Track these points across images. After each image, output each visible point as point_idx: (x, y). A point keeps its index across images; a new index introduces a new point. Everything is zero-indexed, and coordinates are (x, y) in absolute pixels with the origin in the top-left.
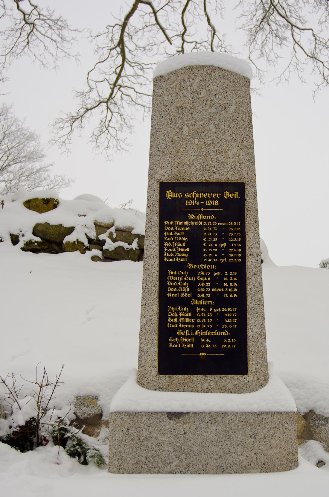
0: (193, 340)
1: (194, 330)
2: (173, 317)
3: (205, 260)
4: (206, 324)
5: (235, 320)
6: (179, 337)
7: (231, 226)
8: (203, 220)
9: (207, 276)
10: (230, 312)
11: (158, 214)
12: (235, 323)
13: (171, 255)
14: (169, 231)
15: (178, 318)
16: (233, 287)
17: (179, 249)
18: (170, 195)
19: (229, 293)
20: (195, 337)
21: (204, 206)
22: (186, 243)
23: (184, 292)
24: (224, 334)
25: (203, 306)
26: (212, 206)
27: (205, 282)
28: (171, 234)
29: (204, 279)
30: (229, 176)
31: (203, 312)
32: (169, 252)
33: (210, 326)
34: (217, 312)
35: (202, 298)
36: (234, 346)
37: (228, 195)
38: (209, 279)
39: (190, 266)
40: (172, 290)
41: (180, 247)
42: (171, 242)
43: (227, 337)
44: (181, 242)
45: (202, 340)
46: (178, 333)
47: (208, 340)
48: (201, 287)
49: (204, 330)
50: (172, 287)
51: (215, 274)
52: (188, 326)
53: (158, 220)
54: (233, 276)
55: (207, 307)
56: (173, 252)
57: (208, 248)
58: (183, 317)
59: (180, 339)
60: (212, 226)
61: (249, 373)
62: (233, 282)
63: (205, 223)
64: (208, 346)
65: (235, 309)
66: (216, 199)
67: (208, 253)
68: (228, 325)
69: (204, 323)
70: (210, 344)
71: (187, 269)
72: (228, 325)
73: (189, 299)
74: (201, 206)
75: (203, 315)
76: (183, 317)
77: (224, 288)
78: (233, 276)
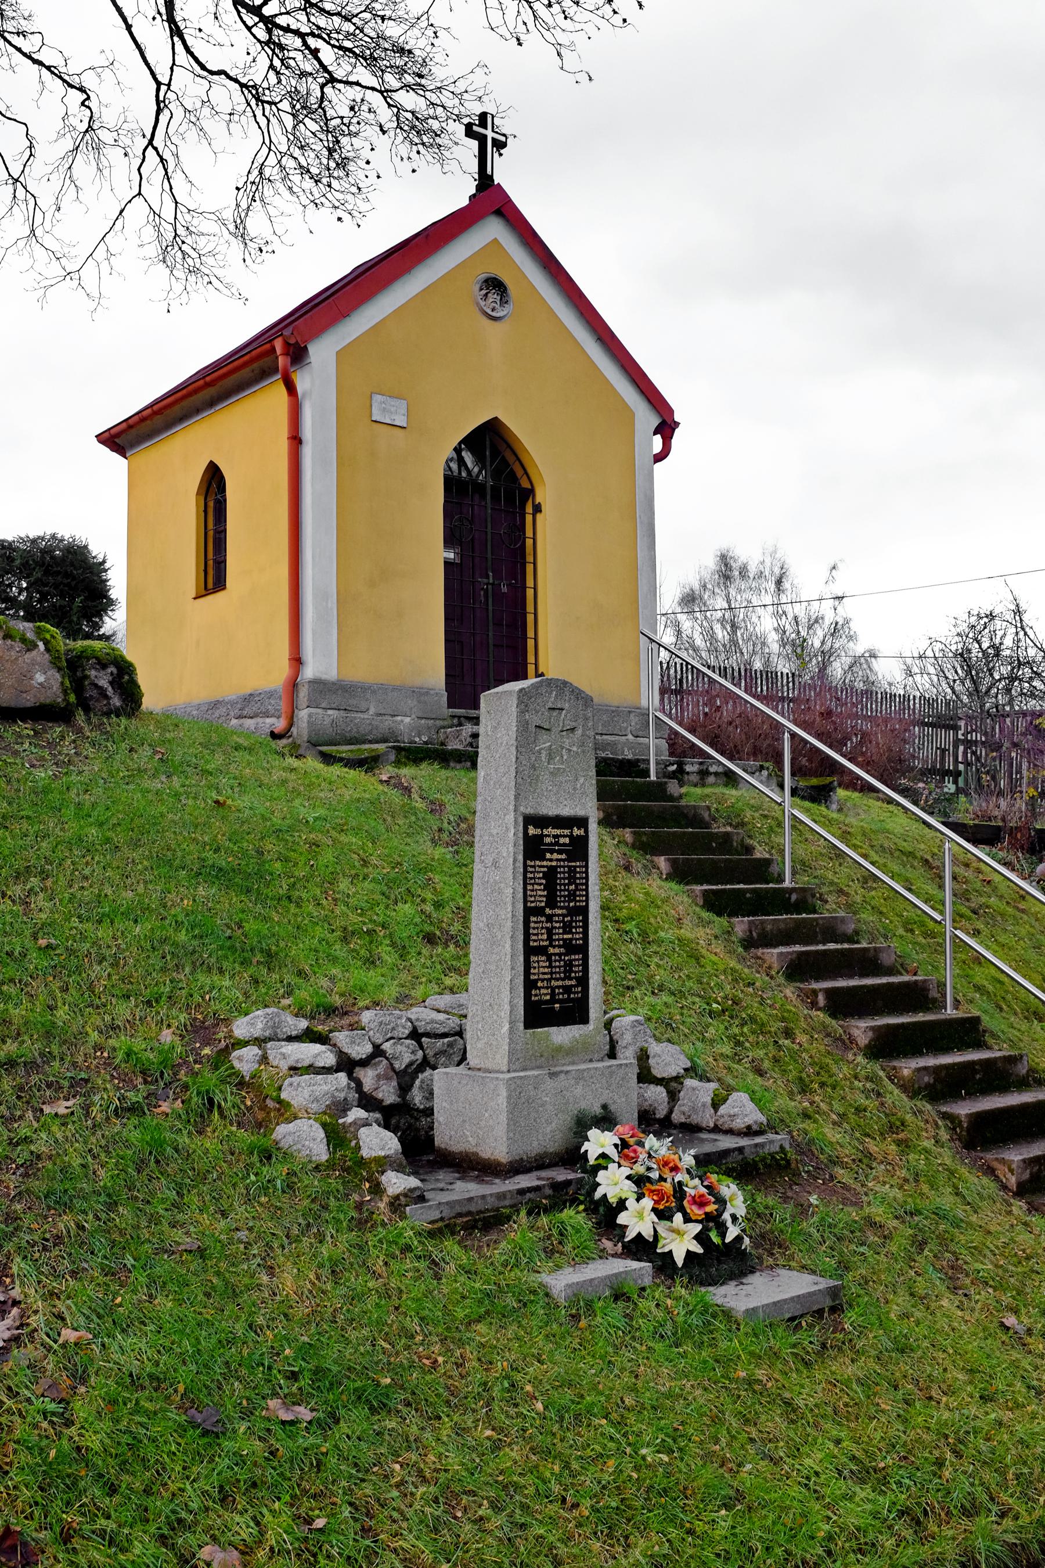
8: (557, 860)
17: (539, 893)
18: (532, 831)
19: (576, 939)
21: (557, 843)
26: (564, 845)
29: (557, 925)
33: (562, 975)
37: (576, 832)
39: (548, 911)
44: (540, 884)
49: (557, 979)
55: (560, 955)
60: (564, 867)
61: (591, 1022)
71: (543, 914)
73: (546, 947)
74: (557, 843)
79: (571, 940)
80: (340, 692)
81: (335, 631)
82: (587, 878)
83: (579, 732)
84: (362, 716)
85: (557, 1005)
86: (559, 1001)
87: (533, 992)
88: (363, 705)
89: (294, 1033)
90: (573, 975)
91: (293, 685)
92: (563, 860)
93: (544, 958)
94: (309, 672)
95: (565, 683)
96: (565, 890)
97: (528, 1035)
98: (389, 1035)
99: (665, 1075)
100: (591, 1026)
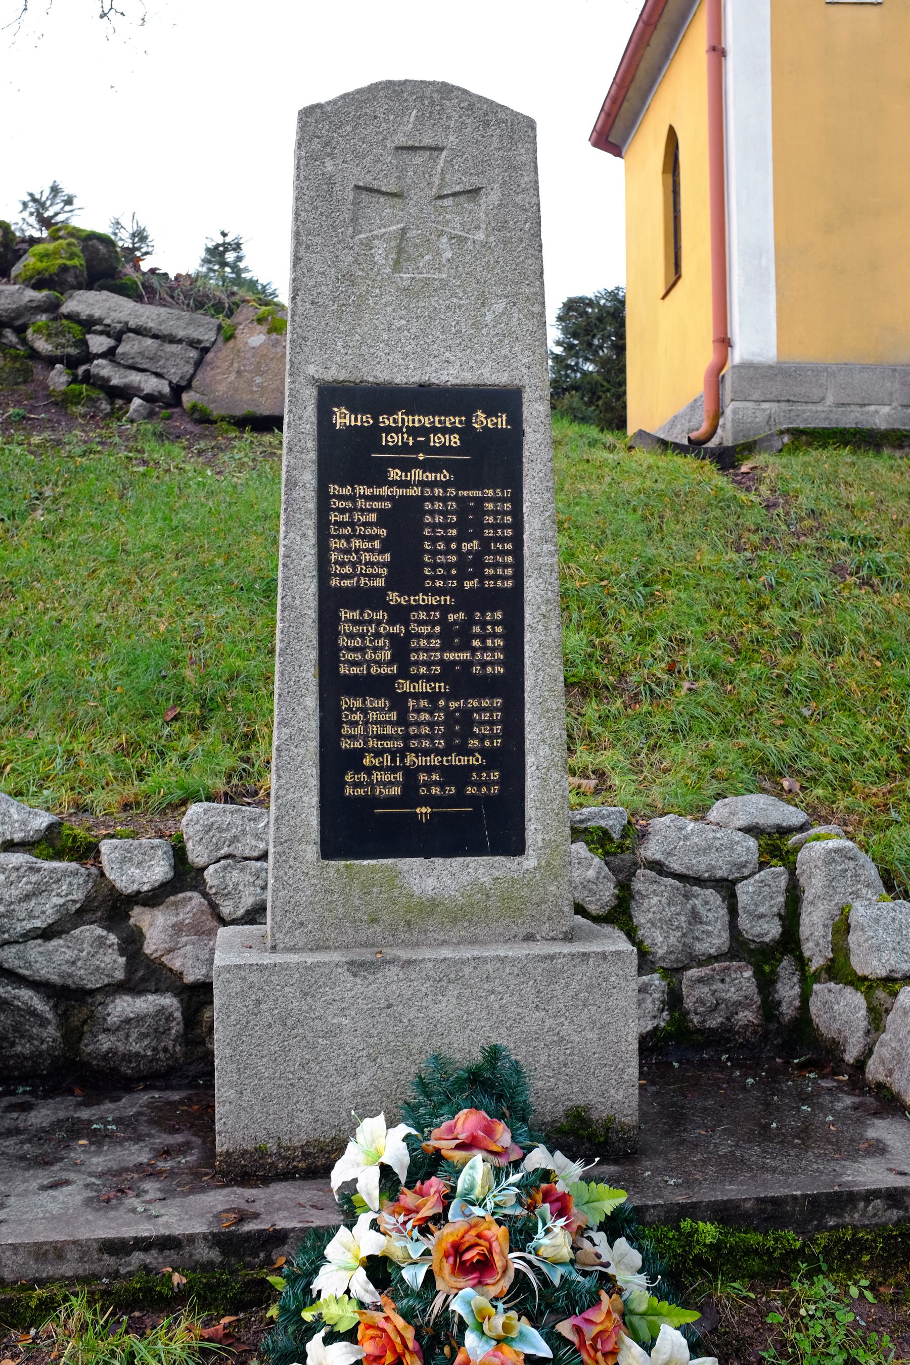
0: (400, 776)
1: (402, 753)
2: (354, 724)
3: (428, 583)
4: (431, 737)
5: (498, 729)
6: (369, 770)
7: (489, 500)
8: (423, 484)
9: (433, 623)
10: (485, 710)
11: (314, 467)
12: (497, 736)
13: (348, 570)
14: (342, 511)
15: (366, 723)
16: (493, 650)
17: (366, 557)
18: (342, 418)
19: (484, 664)
20: (406, 770)
21: (424, 447)
22: (383, 541)
23: (379, 663)
24: (473, 761)
25: (425, 695)
26: (444, 449)
27: (429, 637)
28: (346, 518)
30: (486, 371)
31: (424, 710)
32: (343, 564)
33: (441, 744)
34: (457, 709)
35: (423, 676)
36: (495, 790)
37: (481, 420)
38: (438, 629)
39: (393, 597)
40: (350, 656)
41: (367, 550)
42: (348, 538)
43: (479, 769)
44: (372, 538)
45: (422, 777)
46: (367, 762)
47: (435, 777)
48: (417, 650)
49: (426, 753)
50: (349, 649)
51: (451, 617)
52: (389, 744)
53: (314, 482)
54: (494, 623)
55: (433, 697)
56: (354, 565)
57: (434, 553)
58: (376, 723)
59: (370, 775)
60: (444, 500)
61: (529, 851)
62: (494, 636)
63: (428, 492)
64: (436, 791)
65: (498, 702)
66: (452, 430)
67: (434, 566)
68: (482, 740)
69: (426, 736)
70: (441, 785)
71: (386, 606)
72: (482, 740)
73: (392, 679)
74: (419, 447)
75: (425, 716)
76: (376, 723)
77: (474, 650)
78: (494, 623)
79: (467, 665)
80: (779, 378)
81: (772, 297)
82: (518, 525)
83: (492, 197)
84: (813, 408)
85: (423, 810)
86: (429, 801)
87: (348, 778)
88: (816, 394)
89: (18, 837)
90: (474, 743)
91: (716, 378)
92: (444, 485)
93: (382, 703)
94: (737, 355)
95: (446, 90)
96: (448, 552)
97: (332, 872)
98: (225, 851)
99: (867, 972)
100: (530, 861)
